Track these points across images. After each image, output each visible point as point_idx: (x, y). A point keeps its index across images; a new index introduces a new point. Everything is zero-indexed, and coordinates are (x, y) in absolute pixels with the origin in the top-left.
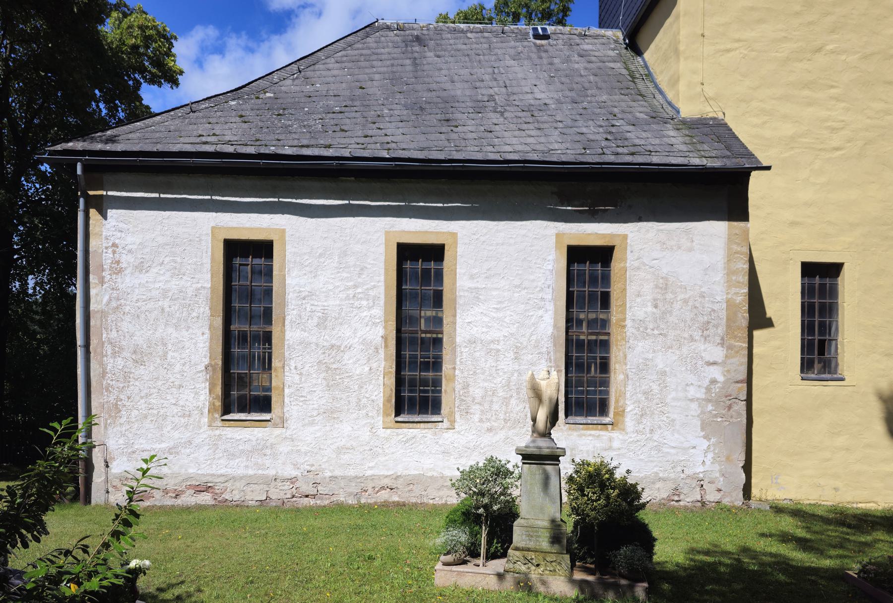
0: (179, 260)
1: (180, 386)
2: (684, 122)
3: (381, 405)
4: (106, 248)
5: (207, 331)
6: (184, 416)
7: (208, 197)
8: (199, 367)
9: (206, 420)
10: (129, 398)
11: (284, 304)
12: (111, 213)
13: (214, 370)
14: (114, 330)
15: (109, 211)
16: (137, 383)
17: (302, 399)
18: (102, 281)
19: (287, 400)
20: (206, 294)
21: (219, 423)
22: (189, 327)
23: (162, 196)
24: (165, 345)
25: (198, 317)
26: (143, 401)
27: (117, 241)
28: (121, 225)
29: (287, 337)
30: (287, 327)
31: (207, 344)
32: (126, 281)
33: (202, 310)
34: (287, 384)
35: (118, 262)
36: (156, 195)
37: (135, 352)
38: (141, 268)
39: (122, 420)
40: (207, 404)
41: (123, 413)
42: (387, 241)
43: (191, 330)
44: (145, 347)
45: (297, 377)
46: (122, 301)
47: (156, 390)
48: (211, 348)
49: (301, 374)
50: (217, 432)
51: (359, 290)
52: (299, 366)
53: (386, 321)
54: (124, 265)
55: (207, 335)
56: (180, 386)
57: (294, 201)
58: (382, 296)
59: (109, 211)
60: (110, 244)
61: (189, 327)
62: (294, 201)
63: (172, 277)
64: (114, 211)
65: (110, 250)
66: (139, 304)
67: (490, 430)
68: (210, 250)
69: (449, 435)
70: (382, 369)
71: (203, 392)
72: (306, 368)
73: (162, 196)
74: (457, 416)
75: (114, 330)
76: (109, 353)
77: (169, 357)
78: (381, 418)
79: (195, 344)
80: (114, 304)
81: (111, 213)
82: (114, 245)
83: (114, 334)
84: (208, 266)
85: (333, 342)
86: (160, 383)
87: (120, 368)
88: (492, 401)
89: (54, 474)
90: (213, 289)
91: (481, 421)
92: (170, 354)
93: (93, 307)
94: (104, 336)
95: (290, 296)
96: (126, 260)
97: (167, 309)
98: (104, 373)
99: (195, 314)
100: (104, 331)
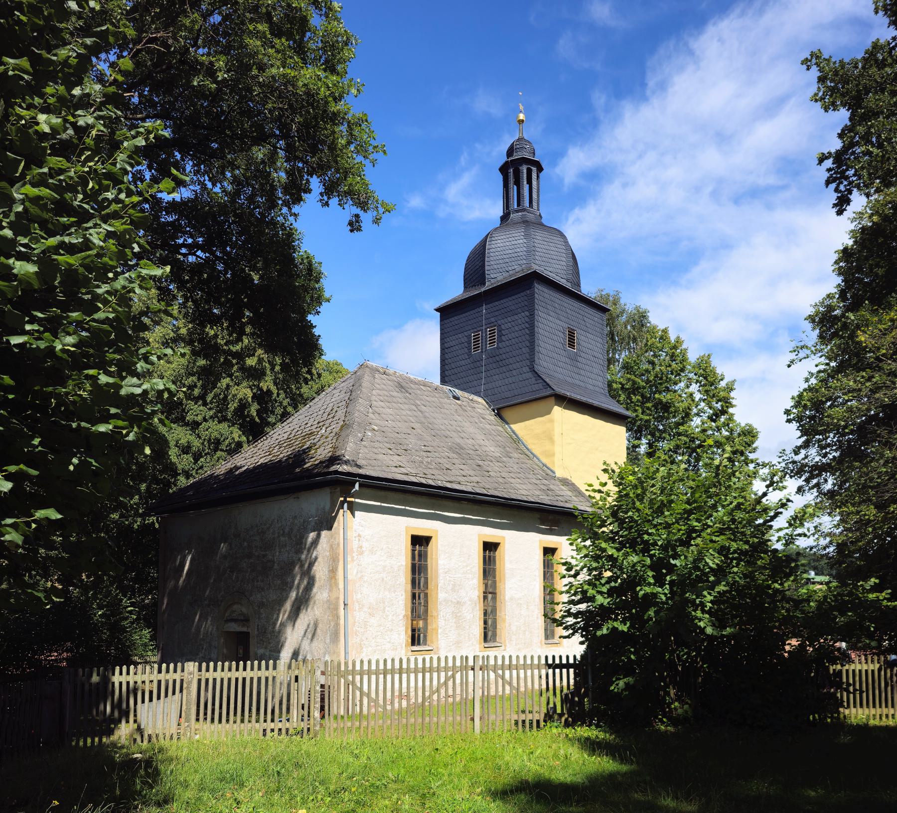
6: (393, 650)
7: (403, 507)
12: (357, 513)
18: (353, 560)
20: (403, 568)
23: (383, 504)
24: (384, 603)
27: (361, 533)
28: (362, 522)
35: (361, 547)
36: (379, 504)
37: (370, 608)
54: (364, 549)
56: (392, 630)
73: (383, 504)
80: (359, 575)
81: (357, 513)
82: (359, 536)
83: (359, 596)
84: (404, 551)
92: (387, 609)
93: (350, 577)
96: (366, 545)
97: (385, 579)
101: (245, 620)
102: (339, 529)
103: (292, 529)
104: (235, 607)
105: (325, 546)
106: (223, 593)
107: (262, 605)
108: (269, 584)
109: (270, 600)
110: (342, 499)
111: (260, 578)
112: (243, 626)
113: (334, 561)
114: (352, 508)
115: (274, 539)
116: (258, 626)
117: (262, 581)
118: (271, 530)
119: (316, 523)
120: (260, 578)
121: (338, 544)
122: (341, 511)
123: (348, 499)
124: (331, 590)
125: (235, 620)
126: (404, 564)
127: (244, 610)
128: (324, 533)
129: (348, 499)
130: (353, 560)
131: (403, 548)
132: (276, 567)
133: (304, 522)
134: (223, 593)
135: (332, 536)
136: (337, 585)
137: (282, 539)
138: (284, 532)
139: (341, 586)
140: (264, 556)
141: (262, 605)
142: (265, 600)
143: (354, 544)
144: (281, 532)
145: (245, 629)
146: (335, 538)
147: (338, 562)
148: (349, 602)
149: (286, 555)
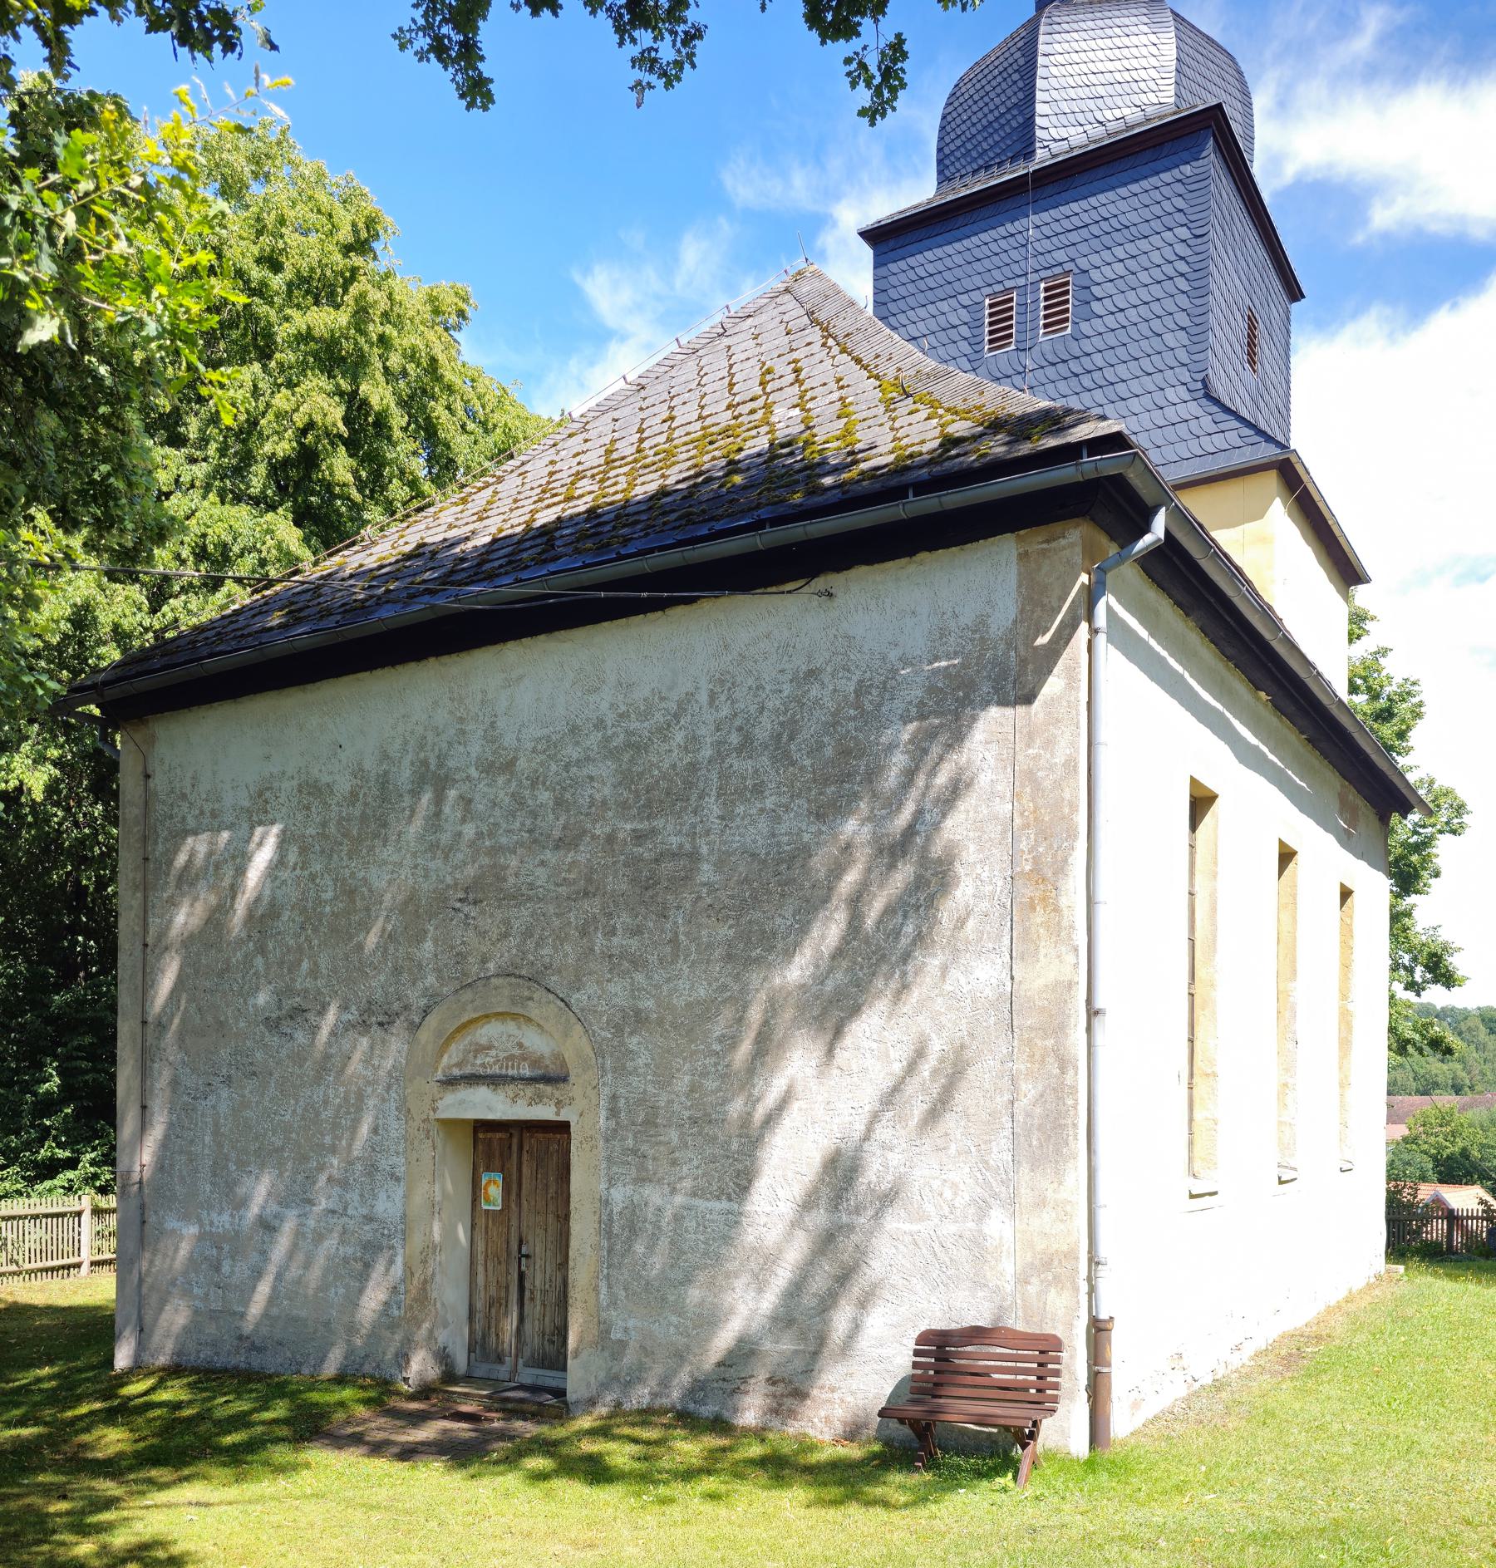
23: (1153, 642)
36: (1143, 633)
103: (791, 728)
104: (489, 1032)
108: (674, 941)
109: (679, 1002)
111: (623, 919)
112: (538, 1099)
113: (1044, 834)
115: (693, 767)
116: (614, 1098)
117: (637, 932)
119: (932, 690)
120: (623, 919)
125: (494, 1081)
133: (862, 689)
134: (431, 980)
139: (1081, 939)
142: (648, 1004)
144: (735, 739)
146: (1049, 744)
149: (763, 825)
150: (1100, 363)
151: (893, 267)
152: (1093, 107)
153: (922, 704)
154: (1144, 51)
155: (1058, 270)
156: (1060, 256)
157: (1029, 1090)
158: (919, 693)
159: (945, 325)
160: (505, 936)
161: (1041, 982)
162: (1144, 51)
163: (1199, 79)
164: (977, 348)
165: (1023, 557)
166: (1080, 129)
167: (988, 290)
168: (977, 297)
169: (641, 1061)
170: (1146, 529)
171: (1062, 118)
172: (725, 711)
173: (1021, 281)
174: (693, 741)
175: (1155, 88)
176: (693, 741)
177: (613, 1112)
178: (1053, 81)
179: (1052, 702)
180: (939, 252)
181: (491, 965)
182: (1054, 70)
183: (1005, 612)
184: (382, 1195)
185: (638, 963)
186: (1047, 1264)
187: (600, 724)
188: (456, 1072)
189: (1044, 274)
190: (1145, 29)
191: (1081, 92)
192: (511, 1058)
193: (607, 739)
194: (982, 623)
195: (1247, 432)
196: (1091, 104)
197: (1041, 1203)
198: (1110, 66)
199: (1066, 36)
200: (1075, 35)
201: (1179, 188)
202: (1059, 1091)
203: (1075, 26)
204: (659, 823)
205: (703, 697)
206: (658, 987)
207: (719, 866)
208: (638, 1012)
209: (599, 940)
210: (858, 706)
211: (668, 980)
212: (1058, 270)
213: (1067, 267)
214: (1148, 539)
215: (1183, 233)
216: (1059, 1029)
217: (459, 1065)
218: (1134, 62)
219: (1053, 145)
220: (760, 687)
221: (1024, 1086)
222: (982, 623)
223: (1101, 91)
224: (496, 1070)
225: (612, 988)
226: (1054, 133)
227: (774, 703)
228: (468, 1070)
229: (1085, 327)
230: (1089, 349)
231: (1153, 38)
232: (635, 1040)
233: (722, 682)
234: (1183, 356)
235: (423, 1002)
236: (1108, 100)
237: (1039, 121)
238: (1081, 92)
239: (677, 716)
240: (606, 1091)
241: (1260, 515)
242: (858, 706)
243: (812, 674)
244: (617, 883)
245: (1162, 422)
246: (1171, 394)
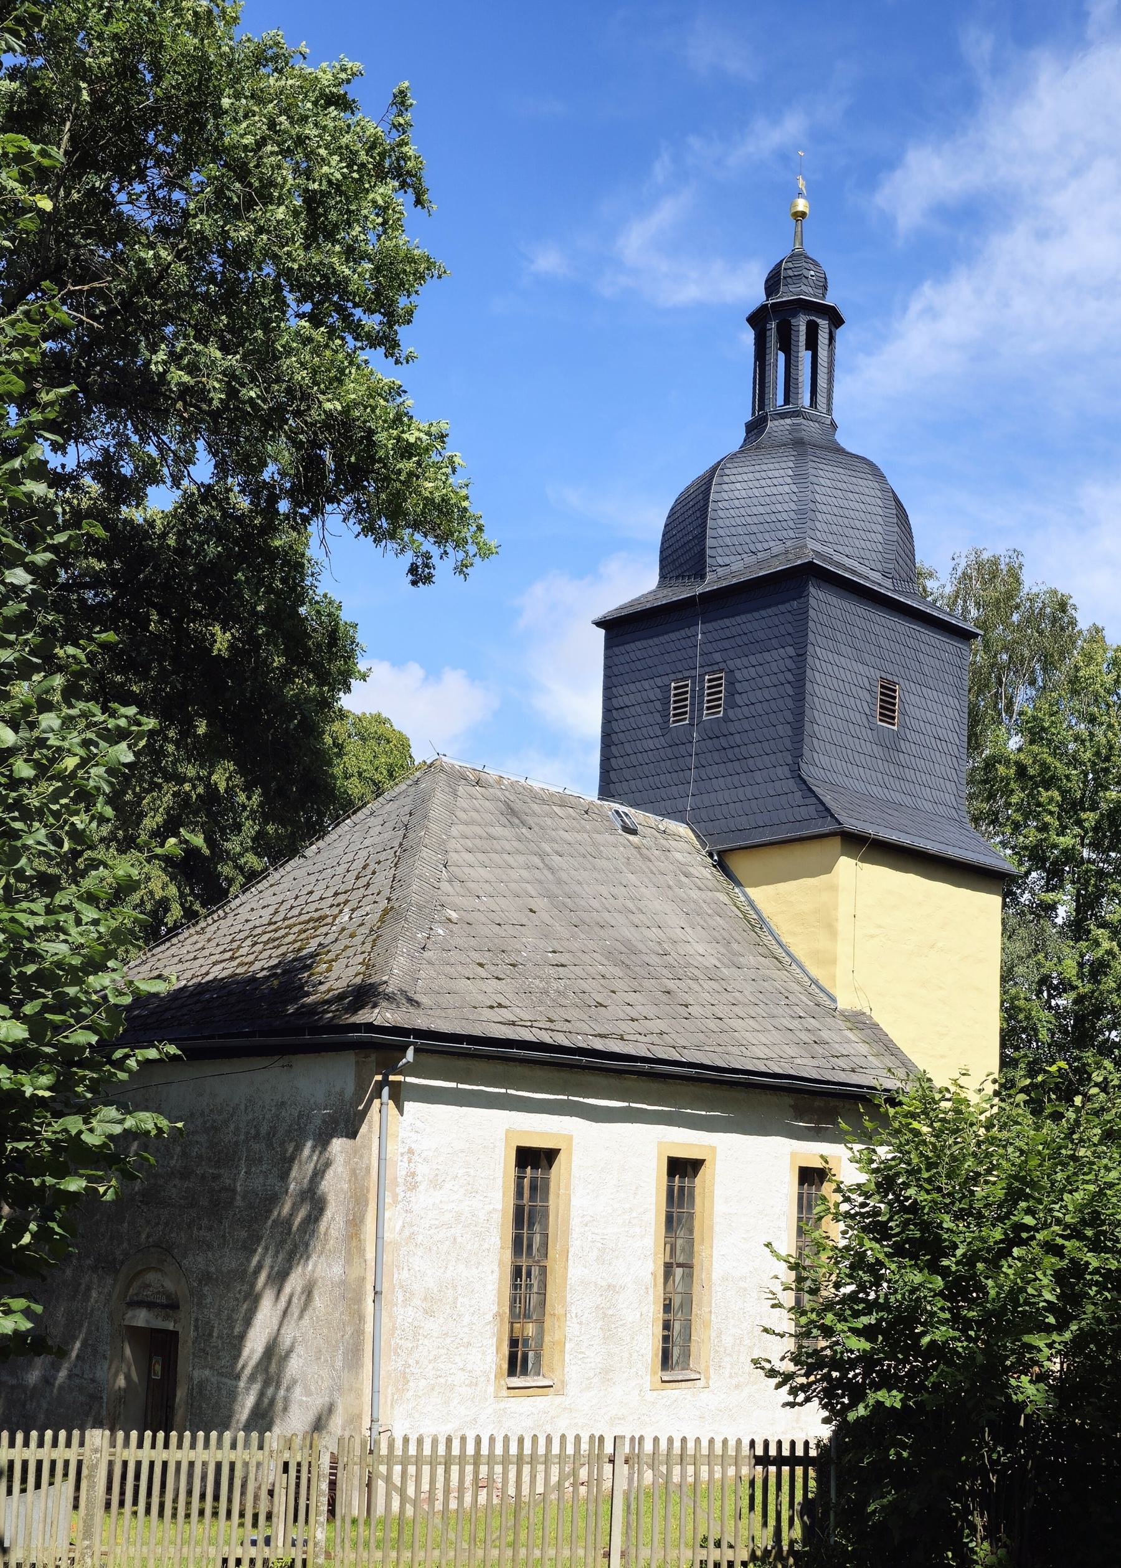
0: (472, 1172)
1: (469, 1344)
2: (842, 1014)
3: (650, 1361)
4: (402, 1154)
5: (497, 1269)
6: (470, 1385)
8: (487, 1317)
9: (491, 1389)
10: (417, 1362)
11: (567, 1232)
13: (502, 1320)
14: (406, 1268)
15: (406, 1103)
16: (426, 1342)
17: (581, 1356)
19: (567, 1357)
20: (497, 1217)
21: (505, 1393)
22: (479, 1263)
24: (455, 1288)
25: (488, 1250)
26: (430, 1366)
27: (413, 1146)
29: (569, 1275)
30: (570, 1262)
31: (496, 1286)
32: (422, 1199)
33: (493, 1239)
34: (569, 1336)
35: (413, 1174)
36: (453, 1085)
37: (425, 1299)
38: (436, 1184)
39: (409, 1395)
40: (494, 1367)
41: (411, 1384)
42: (659, 1154)
43: (480, 1268)
44: (435, 1290)
45: (577, 1327)
46: (415, 1228)
47: (445, 1351)
48: (499, 1291)
49: (581, 1323)
50: (502, 1405)
51: (634, 1214)
52: (580, 1313)
53: (655, 1254)
54: (418, 1179)
55: (496, 1275)
56: (469, 1344)
57: (581, 1100)
58: (653, 1222)
59: (406, 1103)
60: (406, 1150)
61: (479, 1263)
62: (581, 1100)
63: (465, 1195)
64: (411, 1103)
65: (405, 1159)
66: (432, 1231)
67: (737, 1387)
68: (502, 1161)
69: (705, 1395)
70: (651, 1314)
71: (489, 1351)
72: (586, 1315)
74: (712, 1371)
75: (406, 1268)
76: (400, 1301)
77: (459, 1305)
78: (648, 1377)
79: (484, 1286)
80: (407, 1233)
81: (408, 1106)
82: (411, 1151)
83: (405, 1274)
84: (500, 1181)
85: (610, 1281)
86: (448, 1340)
87: (410, 1320)
88: (739, 1352)
89: (980, 1494)
90: (504, 1210)
91: (731, 1376)
92: (460, 1299)
93: (388, 1236)
94: (396, 1276)
95: (575, 1222)
96: (422, 1170)
97: (459, 1240)
98: (394, 1328)
99: (486, 1246)
100: (395, 1270)
101: (171, 1306)
102: (370, 1139)
103: (273, 1130)
104: (151, 1277)
105: (340, 1169)
106: (125, 1245)
107: (206, 1278)
108: (224, 1236)
109: (224, 1269)
110: (379, 1078)
111: (205, 1222)
112: (166, 1318)
113: (357, 1202)
114: (399, 1095)
115: (236, 1143)
116: (197, 1320)
117: (210, 1229)
118: (232, 1127)
119: (324, 1121)
120: (205, 1222)
121: (368, 1169)
122: (377, 1102)
123: (391, 1078)
124: (348, 1262)
125: (150, 1305)
126: (499, 1207)
127: (169, 1285)
128: (338, 1145)
129: (391, 1078)
130: (396, 1202)
131: (499, 1174)
132: (239, 1202)
133: (300, 1116)
134: (125, 1245)
135: (355, 1152)
136: (361, 1251)
137: (256, 1147)
138: (258, 1134)
139: (370, 1255)
140: (216, 1177)
141: (206, 1278)
142: (213, 1269)
143: (399, 1168)
144: (253, 1131)
145: (171, 1326)
146: (361, 1157)
147: (367, 1205)
148: (385, 1287)
149: (261, 1180)
150: (739, 742)
151: (616, 649)
152: (748, 541)
153: (320, 1128)
154: (787, 498)
155: (716, 667)
156: (717, 657)
157: (349, 1330)
158: (320, 1122)
159: (646, 699)
160: (158, 1224)
161: (354, 1276)
162: (787, 498)
163: (835, 510)
164: (666, 719)
165: (357, 1063)
166: (739, 557)
167: (672, 676)
168: (666, 680)
169: (208, 1301)
170: (404, 1057)
171: (726, 550)
172: (250, 1117)
173: (693, 673)
174: (237, 1129)
175: (793, 526)
176: (237, 1129)
177: (196, 1328)
178: (720, 522)
179: (364, 1136)
180: (644, 643)
181: (151, 1240)
182: (720, 513)
183: (350, 1089)
184: (99, 1368)
185: (210, 1247)
186: (352, 1422)
187: (202, 1114)
188: (135, 1298)
189: (707, 669)
190: (789, 480)
191: (740, 530)
192: (158, 1293)
193: (205, 1122)
194: (341, 1093)
195: (821, 808)
196: (747, 539)
197: (350, 1390)
198: (761, 510)
199: (732, 487)
200: (738, 485)
201: (789, 617)
202: (359, 1333)
203: (739, 478)
204: (222, 1171)
205: (242, 1107)
206: (216, 1260)
207: (244, 1198)
208: (208, 1273)
209: (195, 1231)
210: (298, 1124)
211: (221, 1257)
212: (716, 667)
213: (722, 665)
214: (404, 1061)
215: (791, 651)
216: (359, 1299)
217: (137, 1294)
218: (779, 507)
219: (719, 569)
220: (264, 1107)
221: (348, 1329)
222: (341, 1093)
223: (754, 529)
224: (151, 1299)
225: (199, 1259)
226: (720, 560)
227: (268, 1116)
228: (140, 1298)
229: (730, 712)
230: (733, 730)
231: (794, 488)
232: (206, 1288)
233: (250, 1101)
234: (789, 745)
235: (122, 1257)
236: (759, 536)
237: (708, 552)
238: (740, 530)
239: (232, 1116)
240: (194, 1315)
241: (828, 869)
242: (298, 1124)
243: (283, 1103)
244: (204, 1202)
245: (772, 793)
246: (779, 770)
